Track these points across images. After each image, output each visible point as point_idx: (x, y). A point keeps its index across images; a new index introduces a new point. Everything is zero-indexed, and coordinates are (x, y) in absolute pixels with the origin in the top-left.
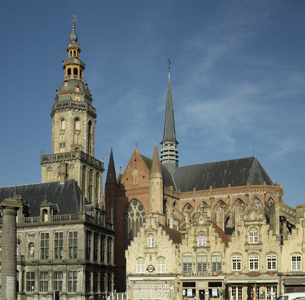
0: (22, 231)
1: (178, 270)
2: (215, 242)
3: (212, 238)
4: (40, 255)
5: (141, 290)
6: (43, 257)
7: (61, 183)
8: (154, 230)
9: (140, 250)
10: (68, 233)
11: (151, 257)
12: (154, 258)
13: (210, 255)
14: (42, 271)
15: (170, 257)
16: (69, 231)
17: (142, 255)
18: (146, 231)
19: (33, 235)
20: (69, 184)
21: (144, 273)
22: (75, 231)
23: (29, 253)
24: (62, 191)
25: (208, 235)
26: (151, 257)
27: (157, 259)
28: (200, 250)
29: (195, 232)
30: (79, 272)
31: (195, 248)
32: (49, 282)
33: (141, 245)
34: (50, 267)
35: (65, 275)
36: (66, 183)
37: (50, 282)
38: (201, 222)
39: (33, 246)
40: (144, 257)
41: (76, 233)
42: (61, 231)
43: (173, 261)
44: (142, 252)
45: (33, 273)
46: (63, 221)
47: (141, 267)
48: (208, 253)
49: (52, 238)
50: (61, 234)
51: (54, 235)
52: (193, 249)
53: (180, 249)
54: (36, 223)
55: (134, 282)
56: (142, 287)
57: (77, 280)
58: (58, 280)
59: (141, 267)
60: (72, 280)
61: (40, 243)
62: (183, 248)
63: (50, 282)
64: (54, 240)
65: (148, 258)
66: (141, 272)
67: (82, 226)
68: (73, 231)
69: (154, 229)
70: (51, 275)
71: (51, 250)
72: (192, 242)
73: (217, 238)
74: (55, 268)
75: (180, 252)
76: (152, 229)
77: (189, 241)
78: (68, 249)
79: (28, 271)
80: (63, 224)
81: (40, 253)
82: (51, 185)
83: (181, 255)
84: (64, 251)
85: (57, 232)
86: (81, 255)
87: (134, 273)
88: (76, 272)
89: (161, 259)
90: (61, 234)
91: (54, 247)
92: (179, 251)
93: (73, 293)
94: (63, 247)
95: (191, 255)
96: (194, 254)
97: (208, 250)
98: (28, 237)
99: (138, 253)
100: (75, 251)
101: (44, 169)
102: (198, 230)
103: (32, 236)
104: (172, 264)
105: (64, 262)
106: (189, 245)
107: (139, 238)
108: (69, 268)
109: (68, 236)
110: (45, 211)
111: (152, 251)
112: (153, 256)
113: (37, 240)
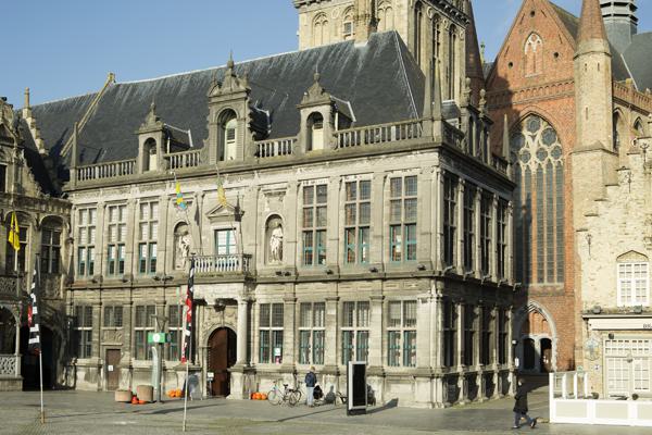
0: (245, 182)
4: (299, 253)
5: (635, 362)
6: (308, 259)
7: (356, 45)
9: (629, 229)
10: (388, 182)
14: (307, 300)
16: (390, 175)
17: (638, 246)
19: (281, 193)
20: (383, 44)
21: (645, 305)
22: (409, 173)
23: (267, 245)
24: (360, 65)
30: (424, 301)
32: (328, 334)
33: (632, 213)
34: (331, 287)
35: (376, 312)
36: (373, 44)
37: (331, 334)
39: (280, 225)
41: (411, 181)
42: (364, 177)
45: (279, 308)
46: (371, 146)
47: (633, 286)
49: (336, 200)
50: (365, 185)
51: (343, 189)
54: (288, 157)
55: (611, 337)
56: (637, 353)
57: (418, 327)
58: (355, 329)
59: (633, 286)
60: (401, 328)
61: (300, 214)
63: (331, 334)
64: (343, 203)
66: (633, 303)
67: (433, 157)
70: (334, 313)
71: (335, 237)
74: (349, 292)
78: (386, 230)
79: (263, 302)
80: (372, 155)
81: (300, 244)
82: (328, 53)
84: (376, 237)
85: (351, 179)
86: (430, 249)
87: (611, 306)
88: (414, 302)
90: (365, 185)
91: (342, 226)
93: (402, 369)
94: (372, 224)
98: (263, 198)
99: (621, 237)
100: (408, 236)
101: (304, 19)
103: (276, 194)
105: (374, 271)
107: (625, 187)
108: (391, 289)
109: (387, 190)
110: (316, 119)
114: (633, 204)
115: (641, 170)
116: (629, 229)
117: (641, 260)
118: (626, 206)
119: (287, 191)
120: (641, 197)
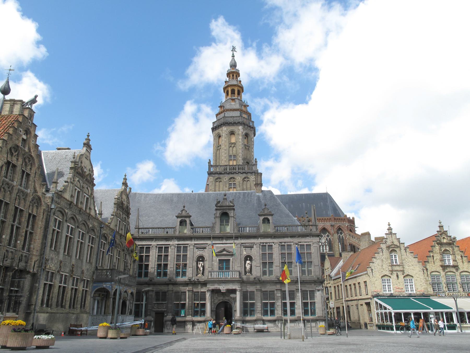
1: (429, 290)
2: (461, 261)
3: (458, 257)
8: (398, 247)
9: (384, 267)
11: (397, 276)
12: (401, 277)
13: (459, 274)
15: (417, 276)
17: (388, 273)
18: (388, 247)
25: (454, 254)
26: (397, 276)
27: (404, 277)
28: (448, 269)
29: (440, 250)
31: (444, 267)
33: (384, 262)
38: (445, 241)
40: (390, 275)
43: (422, 280)
44: (387, 269)
48: (456, 272)
52: (441, 268)
53: (428, 267)
62: (431, 267)
65: (394, 276)
68: (305, 244)
69: (396, 245)
72: (438, 260)
73: (463, 258)
75: (429, 270)
76: (394, 245)
77: (435, 259)
83: (429, 273)
88: (313, 291)
89: (408, 278)
92: (427, 269)
95: (439, 274)
96: (443, 273)
97: (457, 270)
99: (382, 270)
102: (443, 249)
104: (421, 283)
106: (436, 264)
107: (381, 254)
111: (397, 268)
112: (400, 274)
113: (256, 252)
114: (384, 259)
115: (385, 249)
116: (384, 267)
117: (388, 278)
118: (382, 260)
119: (255, 246)
120: (386, 257)
